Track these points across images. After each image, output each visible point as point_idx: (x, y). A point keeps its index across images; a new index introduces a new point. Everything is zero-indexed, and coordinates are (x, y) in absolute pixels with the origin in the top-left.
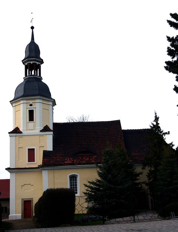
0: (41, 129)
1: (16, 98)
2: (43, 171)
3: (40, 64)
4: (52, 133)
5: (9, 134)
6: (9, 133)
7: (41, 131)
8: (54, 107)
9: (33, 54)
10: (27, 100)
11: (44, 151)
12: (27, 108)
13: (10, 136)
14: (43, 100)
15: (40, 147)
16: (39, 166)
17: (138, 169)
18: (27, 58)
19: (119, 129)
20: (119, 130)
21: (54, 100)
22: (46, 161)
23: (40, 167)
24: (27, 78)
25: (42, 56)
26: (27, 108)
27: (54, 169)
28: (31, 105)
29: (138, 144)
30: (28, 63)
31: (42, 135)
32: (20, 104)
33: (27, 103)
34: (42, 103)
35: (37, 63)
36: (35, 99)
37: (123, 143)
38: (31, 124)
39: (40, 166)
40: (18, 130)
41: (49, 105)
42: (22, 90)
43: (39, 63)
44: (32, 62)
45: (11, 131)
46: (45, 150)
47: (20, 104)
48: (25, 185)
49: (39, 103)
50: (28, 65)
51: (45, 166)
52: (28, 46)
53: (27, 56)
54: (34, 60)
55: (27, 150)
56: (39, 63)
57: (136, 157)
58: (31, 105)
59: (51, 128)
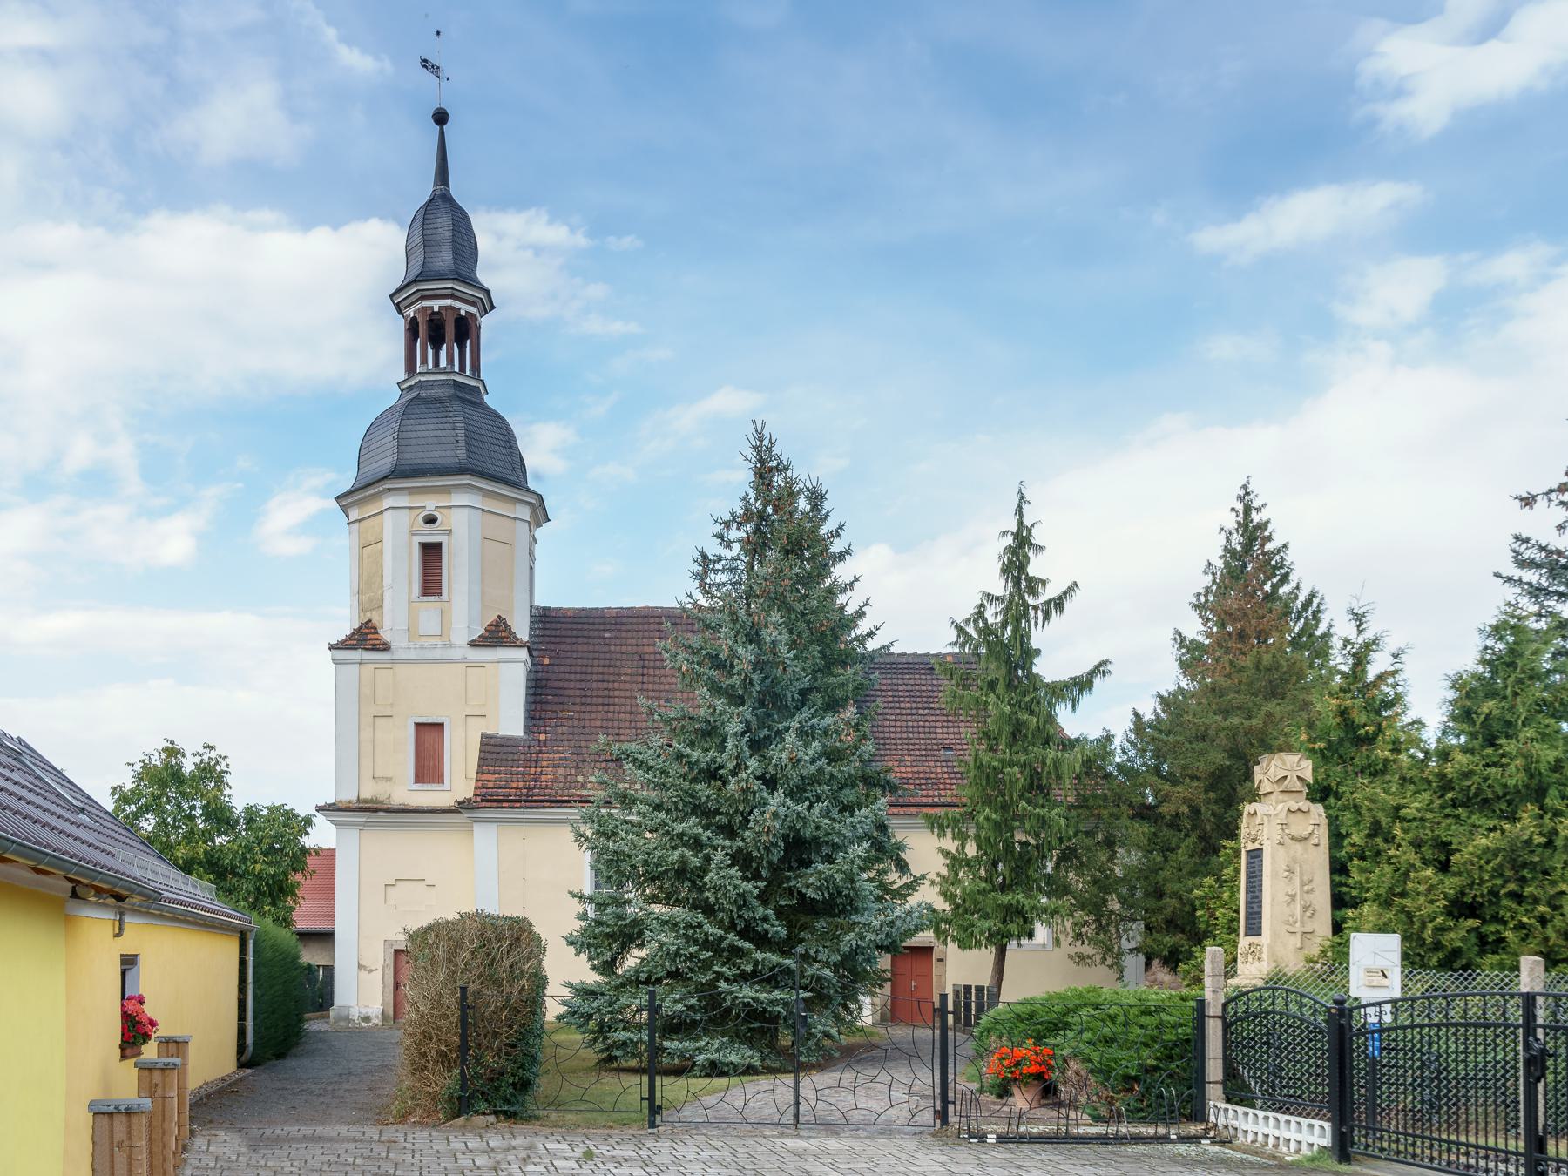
1: (357, 486)
2: (476, 827)
6: (332, 647)
8: (538, 533)
9: (444, 258)
10: (411, 491)
12: (413, 533)
13: (336, 662)
14: (487, 494)
16: (460, 803)
18: (415, 281)
22: (491, 785)
23: (463, 806)
24: (413, 382)
26: (413, 533)
27: (524, 821)
28: (431, 520)
31: (480, 664)
32: (382, 512)
33: (410, 508)
34: (483, 510)
35: (464, 309)
36: (447, 490)
38: (429, 611)
39: (463, 802)
41: (515, 519)
43: (473, 310)
44: (436, 305)
46: (491, 731)
47: (382, 512)
48: (398, 883)
53: (415, 272)
54: (449, 292)
55: (412, 730)
56: (473, 310)
58: (431, 520)
59: (522, 630)
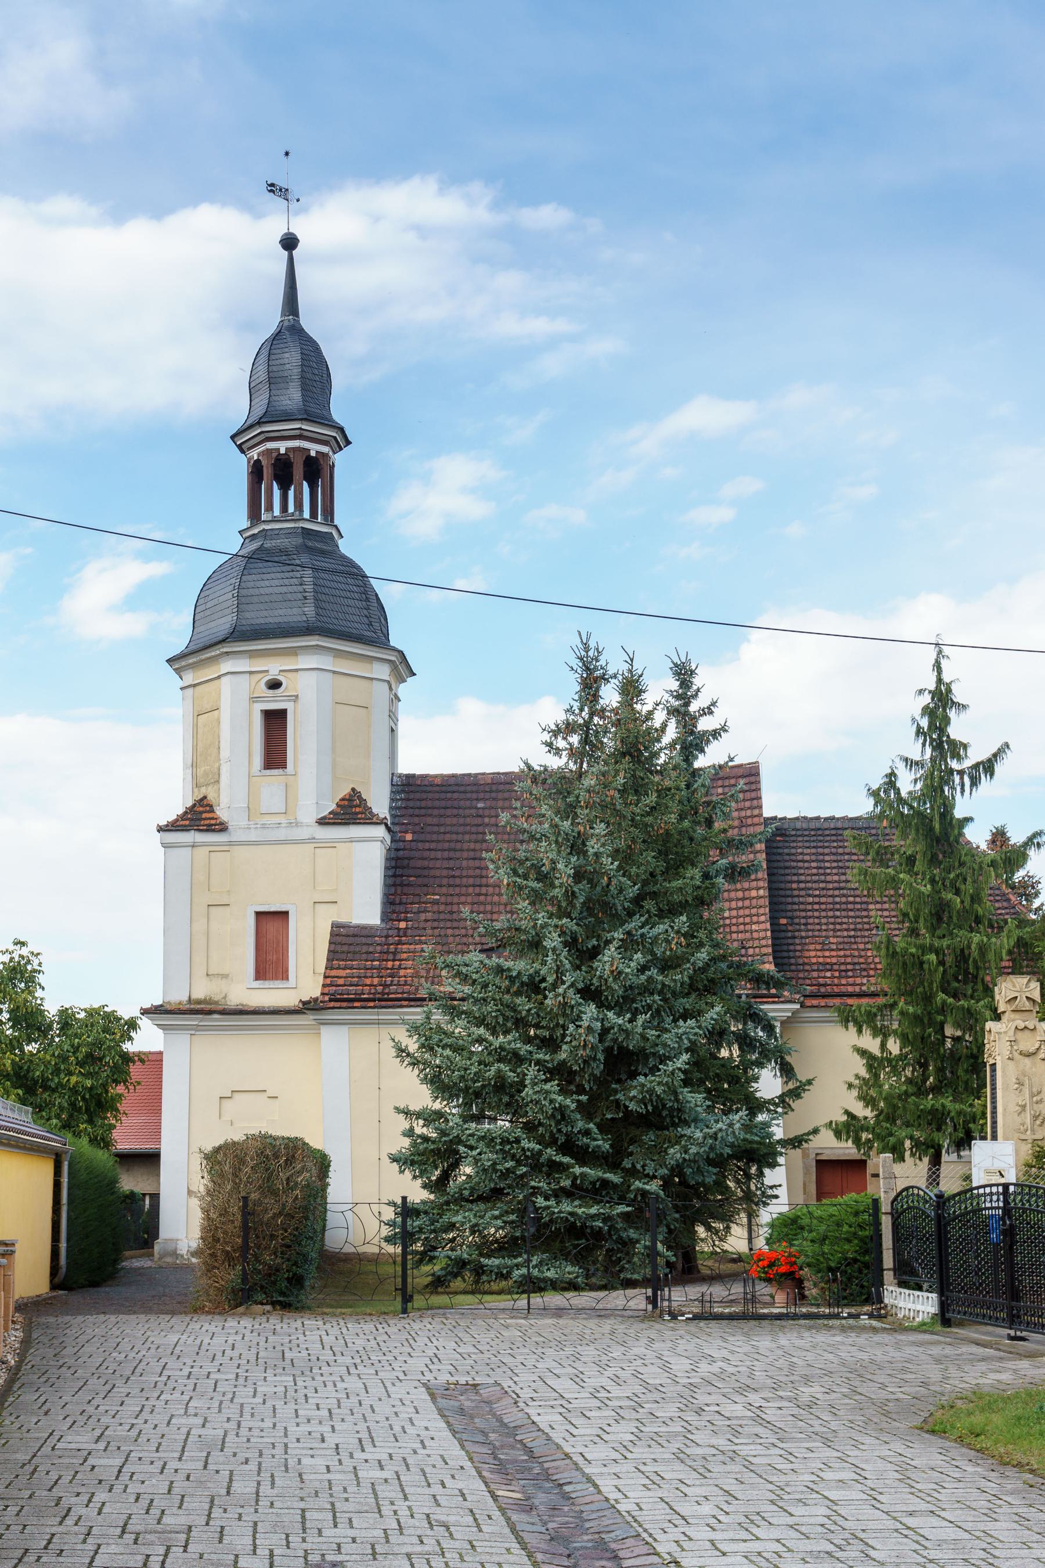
0: (326, 813)
1: (192, 647)
2: (325, 1030)
3: (325, 456)
4: (380, 831)
5: (174, 681)
6: (160, 829)
7: (322, 822)
8: (402, 690)
9: (292, 397)
10: (252, 654)
11: (336, 926)
12: (254, 699)
13: (165, 846)
14: (338, 654)
15: (317, 905)
16: (304, 1003)
17: (724, 1053)
18: (259, 423)
19: (747, 817)
20: (749, 821)
21: (401, 653)
22: (341, 981)
23: (308, 1007)
24: (255, 531)
25: (338, 412)
26: (254, 699)
27: (379, 1023)
28: (275, 685)
29: (851, 899)
30: (261, 448)
31: (331, 844)
32: (219, 677)
33: (251, 673)
34: (334, 672)
35: (314, 449)
36: (293, 652)
37: (761, 892)
38: (274, 780)
39: (309, 1002)
40: (204, 816)
41: (372, 679)
42: (225, 605)
43: (325, 449)
44: (282, 446)
45: (172, 817)
46: (343, 919)
47: (219, 677)
48: (236, 1095)
49: (314, 674)
50: (264, 463)
51: (338, 1004)
52: (265, 353)
53: (259, 411)
54: (297, 432)
55: (251, 920)
56: (325, 449)
57: (828, 974)
58: (275, 685)
59: (380, 803)
